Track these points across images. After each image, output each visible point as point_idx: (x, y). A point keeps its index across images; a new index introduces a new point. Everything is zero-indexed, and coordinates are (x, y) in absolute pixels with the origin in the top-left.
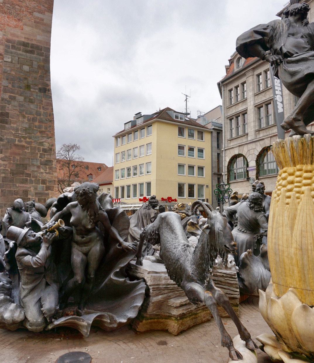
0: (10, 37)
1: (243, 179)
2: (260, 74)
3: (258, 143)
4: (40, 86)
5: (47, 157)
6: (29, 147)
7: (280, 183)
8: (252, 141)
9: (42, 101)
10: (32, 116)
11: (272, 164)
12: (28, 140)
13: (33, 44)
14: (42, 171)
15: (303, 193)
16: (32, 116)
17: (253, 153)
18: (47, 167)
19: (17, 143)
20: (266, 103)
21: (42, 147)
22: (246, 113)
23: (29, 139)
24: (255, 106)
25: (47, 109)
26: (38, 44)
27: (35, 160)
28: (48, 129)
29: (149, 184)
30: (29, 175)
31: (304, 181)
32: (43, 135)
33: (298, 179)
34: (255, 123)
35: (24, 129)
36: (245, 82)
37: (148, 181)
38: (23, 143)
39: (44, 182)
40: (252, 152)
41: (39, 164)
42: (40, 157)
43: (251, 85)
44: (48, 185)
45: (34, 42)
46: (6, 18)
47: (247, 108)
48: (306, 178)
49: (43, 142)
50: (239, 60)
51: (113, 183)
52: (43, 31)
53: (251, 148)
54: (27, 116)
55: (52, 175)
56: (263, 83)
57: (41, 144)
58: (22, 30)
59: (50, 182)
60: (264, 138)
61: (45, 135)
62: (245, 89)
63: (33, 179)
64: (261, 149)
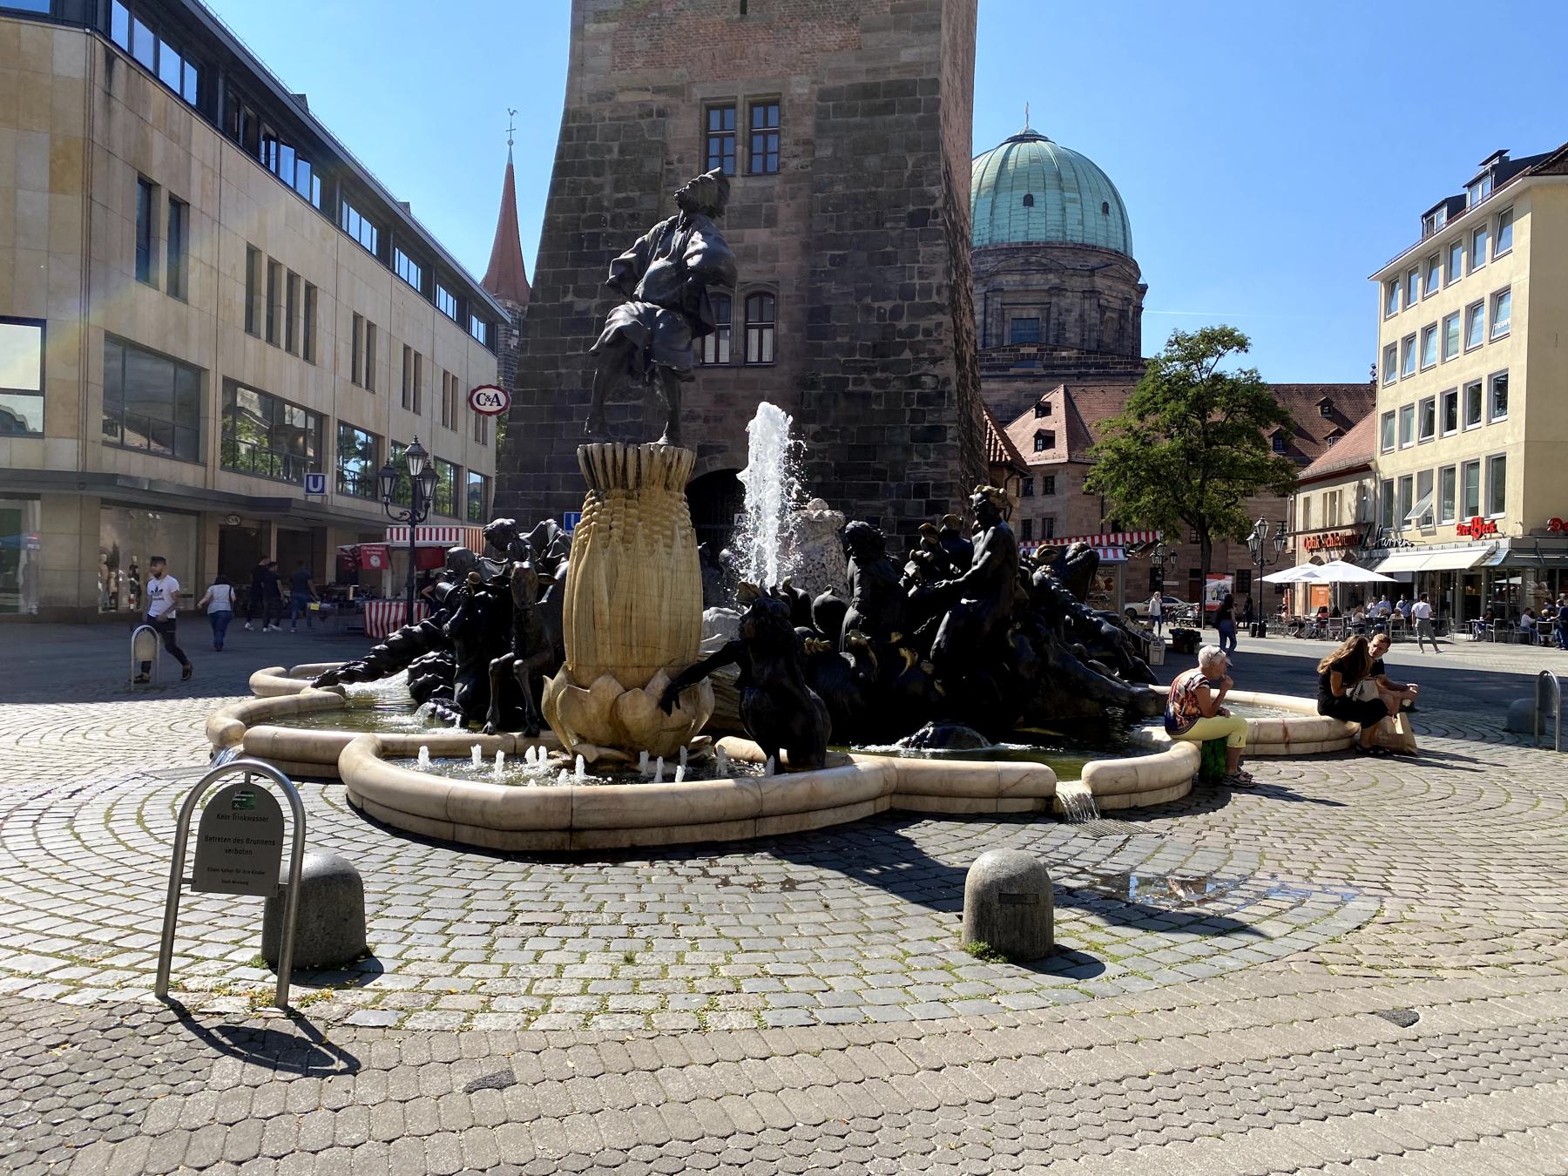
0: (829, 83)
4: (911, 208)
5: (931, 419)
6: (879, 396)
9: (918, 253)
10: (888, 305)
12: (878, 375)
13: (890, 83)
14: (916, 459)
16: (888, 305)
18: (931, 445)
19: (851, 388)
21: (916, 391)
23: (882, 371)
25: (933, 273)
26: (907, 77)
27: (898, 431)
28: (935, 334)
29: (1498, 463)
30: (880, 474)
32: (921, 356)
35: (868, 346)
37: (1496, 450)
38: (868, 388)
39: (921, 490)
41: (907, 437)
42: (910, 422)
44: (931, 498)
45: (893, 76)
46: (817, 30)
49: (920, 375)
51: (1372, 464)
52: (917, 29)
54: (876, 305)
55: (943, 470)
57: (915, 382)
58: (860, 48)
59: (938, 487)
61: (925, 355)
63: (893, 484)
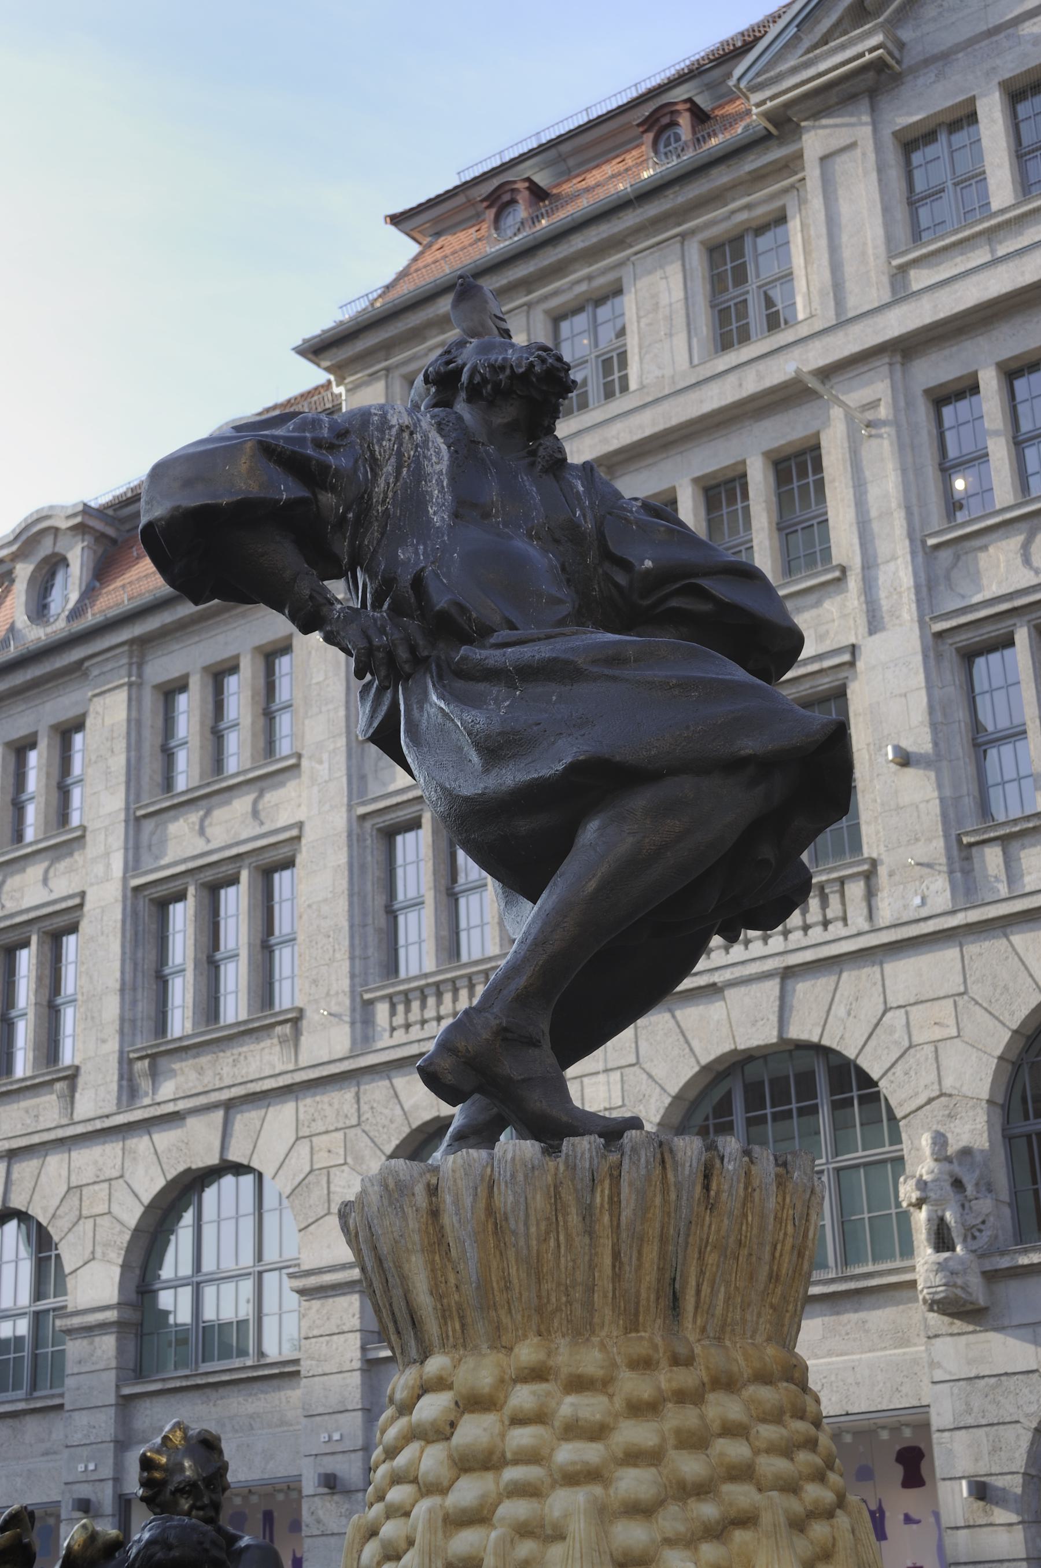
1: (21, 1393)
2: (180, 686)
3: (141, 1144)
7: (402, 1460)
8: (99, 1125)
11: (227, 1288)
15: (559, 1536)
17: (102, 1208)
20: (208, 876)
22: (73, 928)
24: (137, 889)
31: (567, 1454)
33: (522, 1437)
34: (134, 1002)
36: (78, 725)
40: (96, 1201)
43: (121, 745)
47: (83, 894)
48: (573, 1430)
50: (52, 575)
53: (88, 1177)
56: (195, 741)
60: (181, 1106)
62: (77, 768)
64: (160, 1183)
